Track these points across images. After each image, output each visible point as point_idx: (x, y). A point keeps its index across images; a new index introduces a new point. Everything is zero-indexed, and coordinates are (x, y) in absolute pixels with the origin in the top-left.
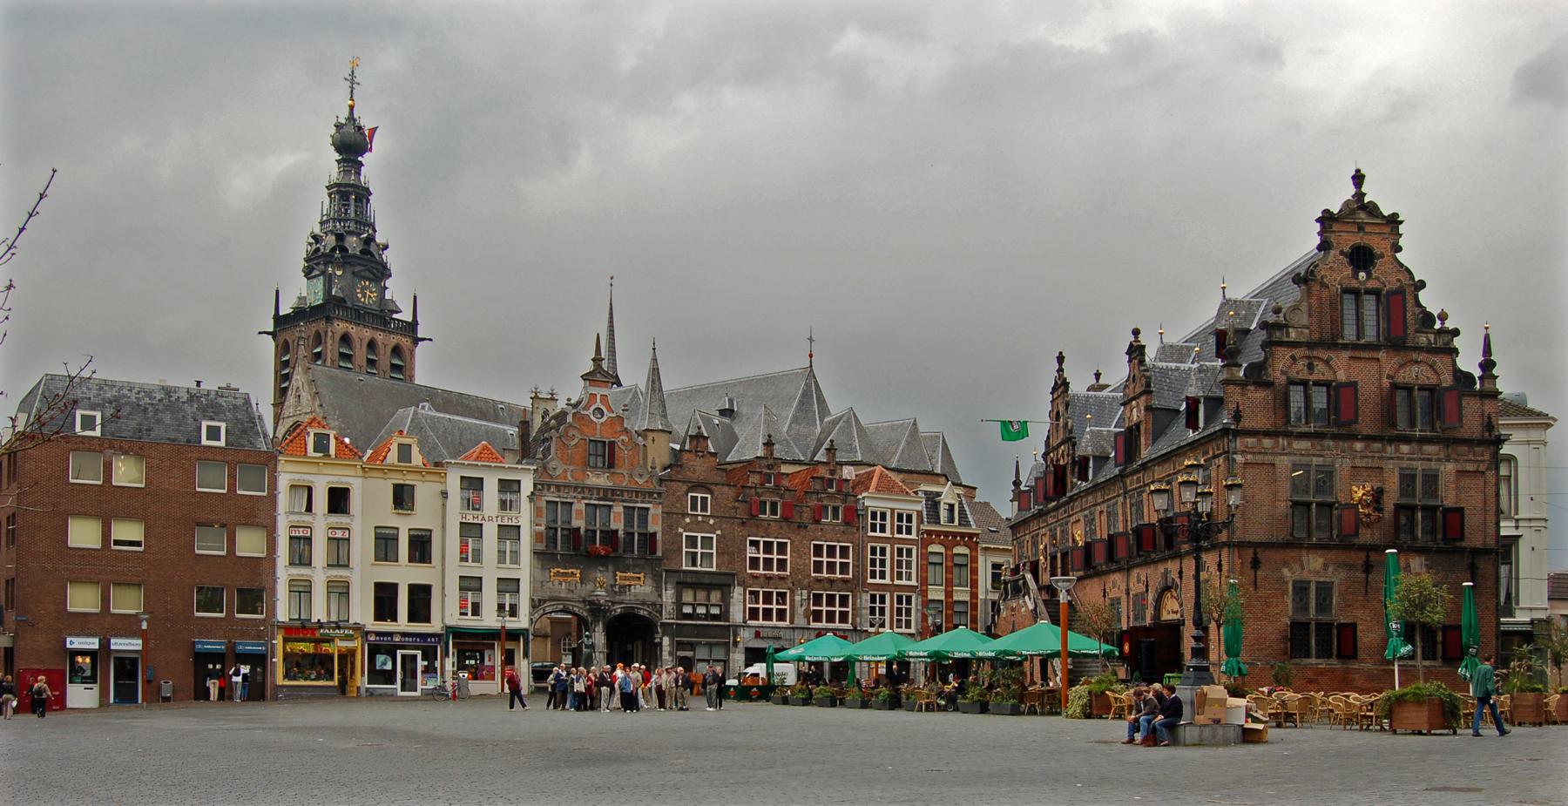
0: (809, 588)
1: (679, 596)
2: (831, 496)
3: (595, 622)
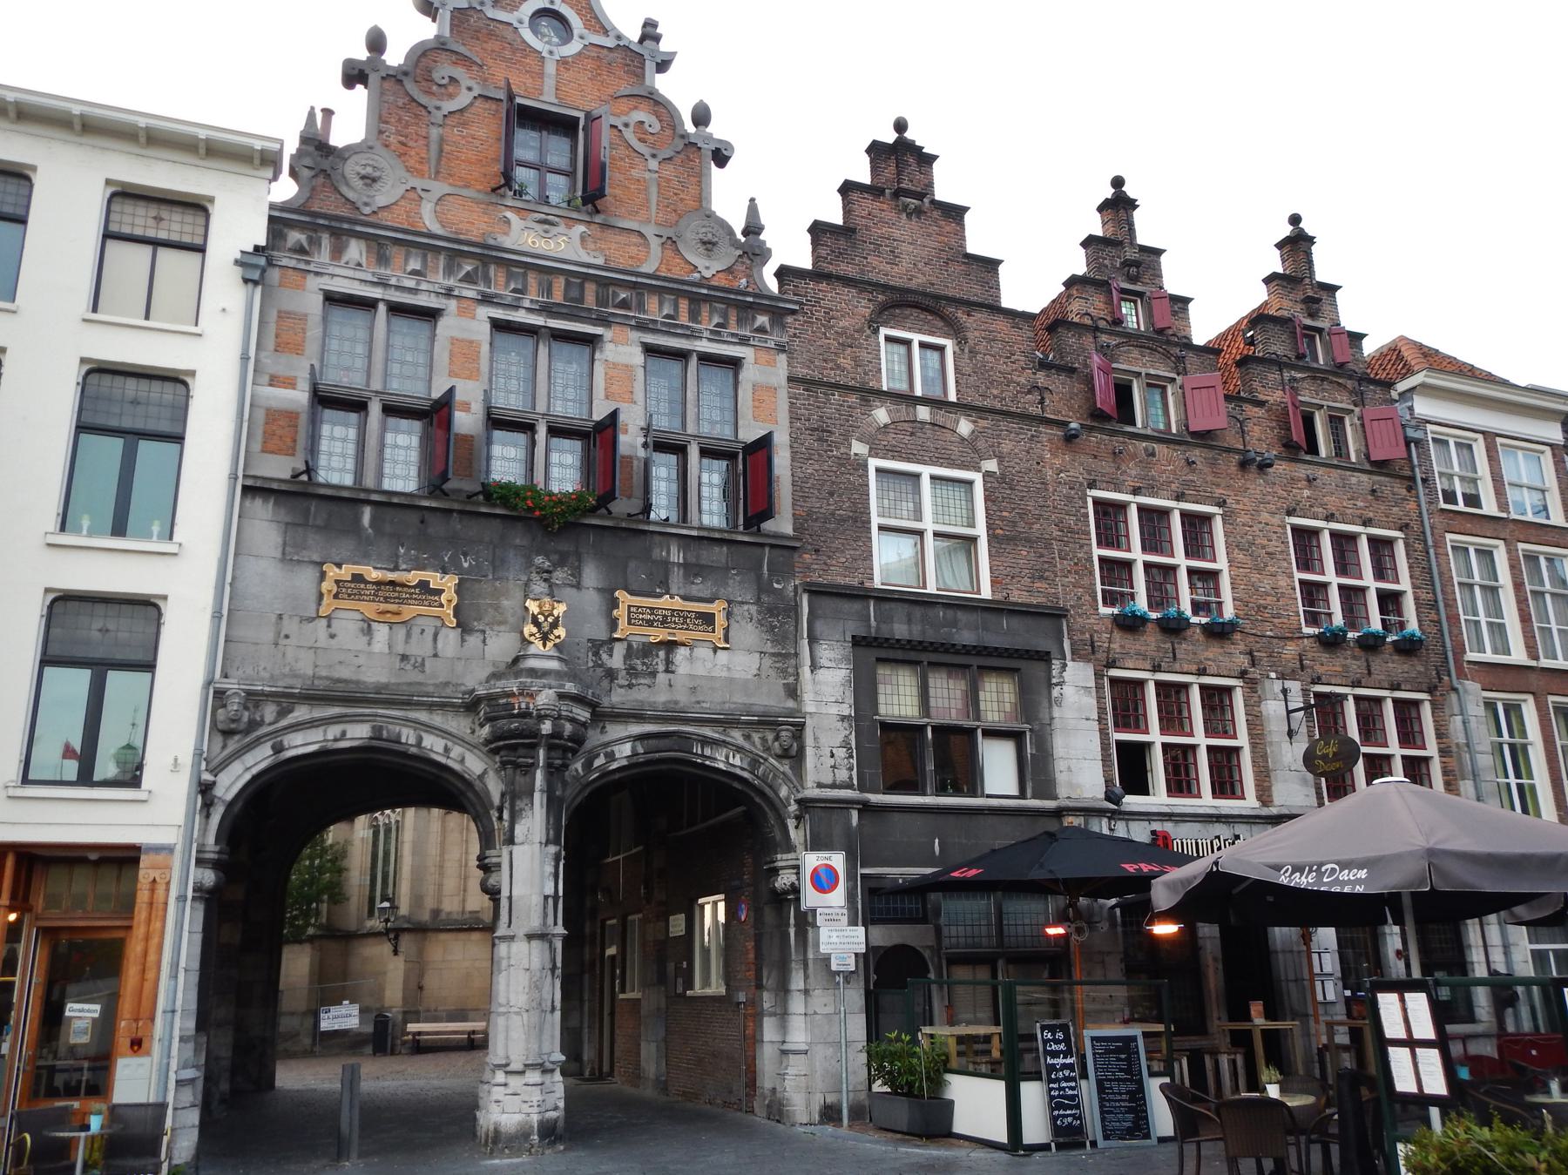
0: (1299, 669)
1: (864, 691)
2: (1318, 376)
3: (516, 796)
